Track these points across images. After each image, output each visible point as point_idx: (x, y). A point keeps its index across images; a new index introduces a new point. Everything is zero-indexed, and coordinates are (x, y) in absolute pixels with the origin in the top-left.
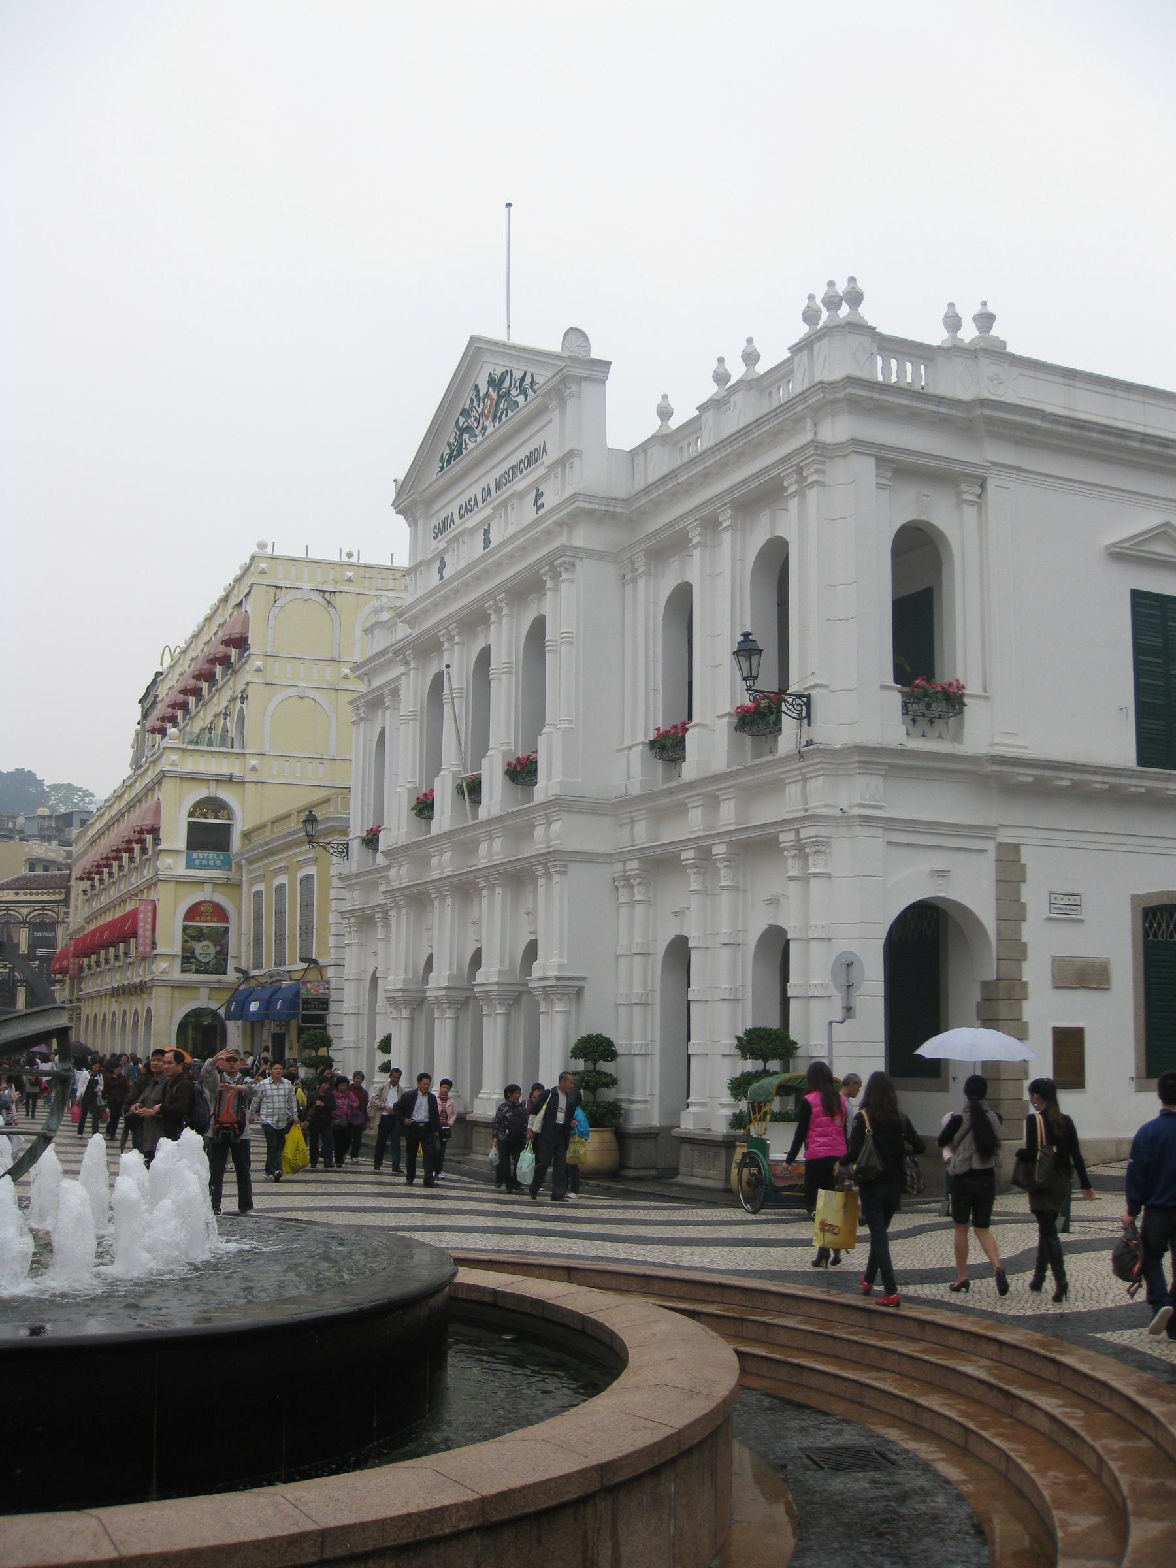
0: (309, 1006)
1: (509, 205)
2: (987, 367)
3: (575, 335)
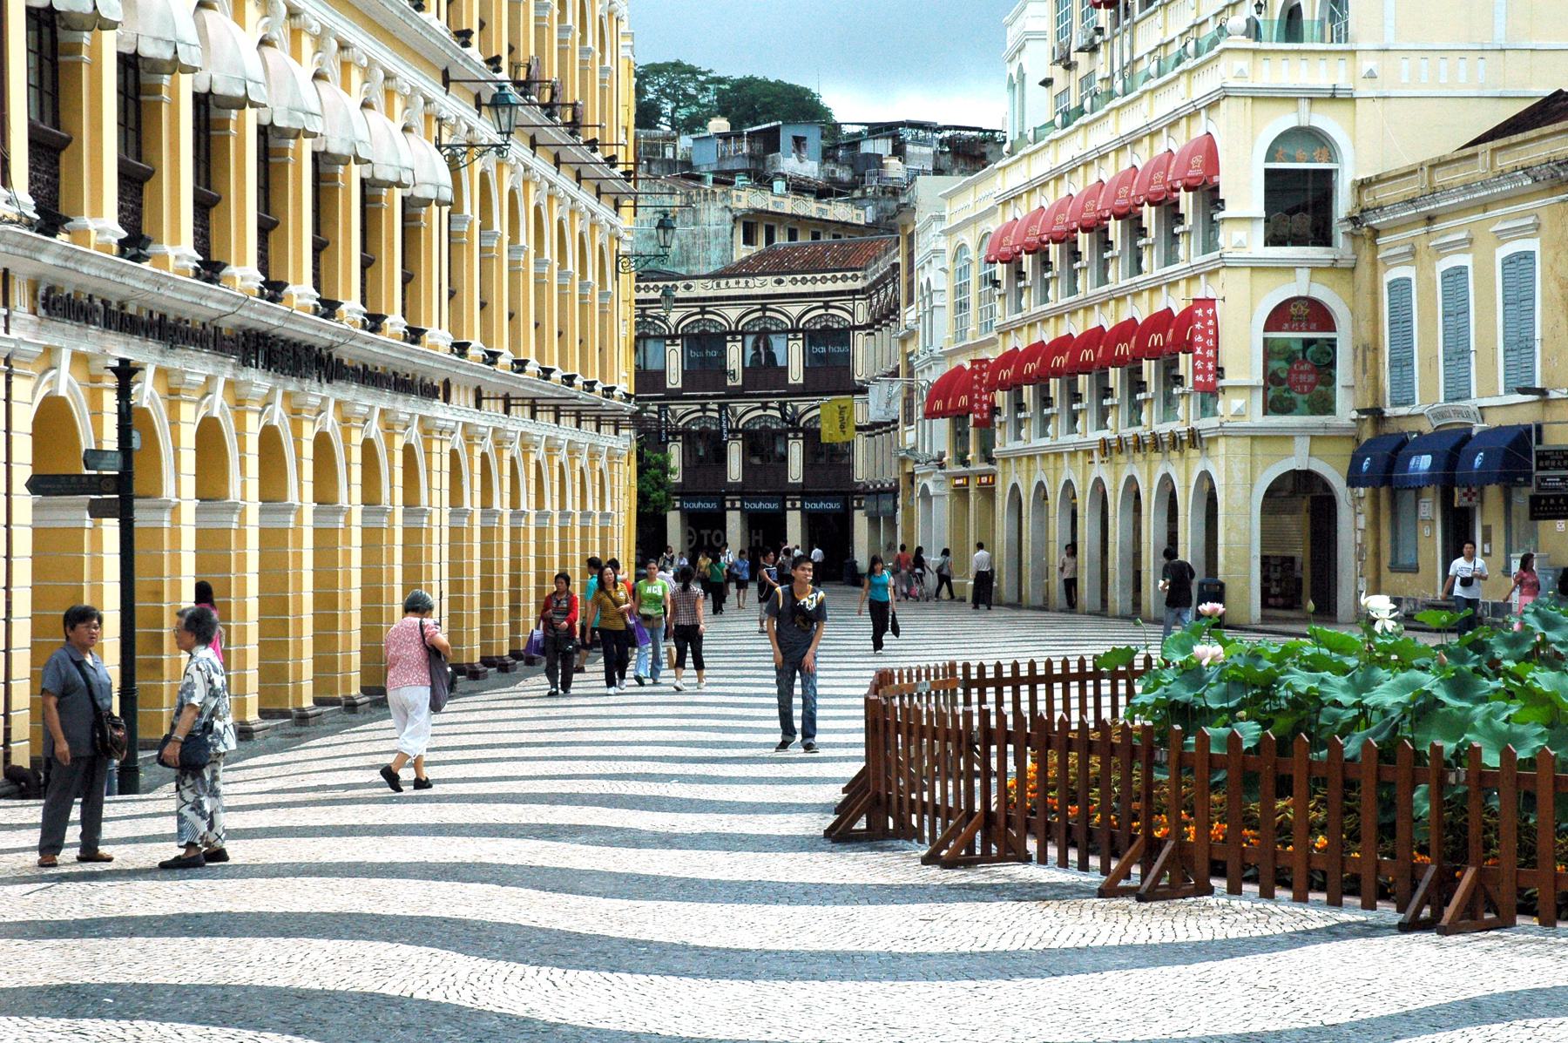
0: (1547, 463)
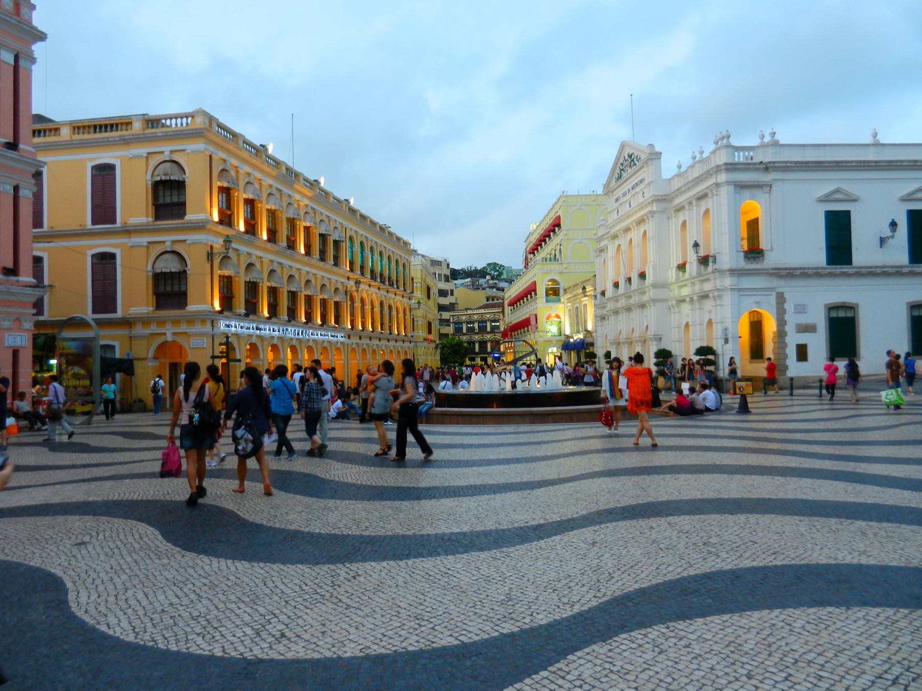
2: (770, 150)
3: (651, 146)
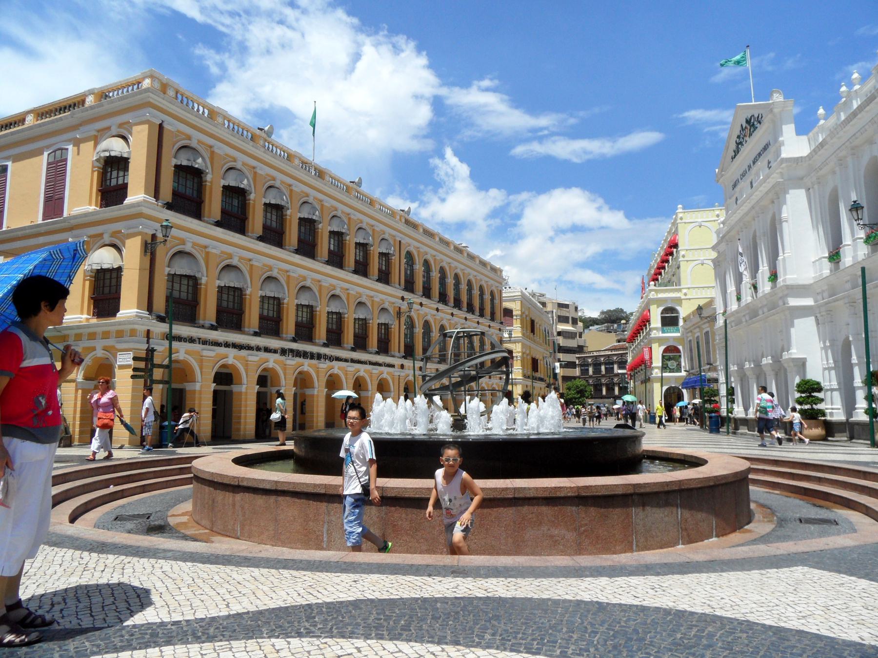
1: (748, 46)
